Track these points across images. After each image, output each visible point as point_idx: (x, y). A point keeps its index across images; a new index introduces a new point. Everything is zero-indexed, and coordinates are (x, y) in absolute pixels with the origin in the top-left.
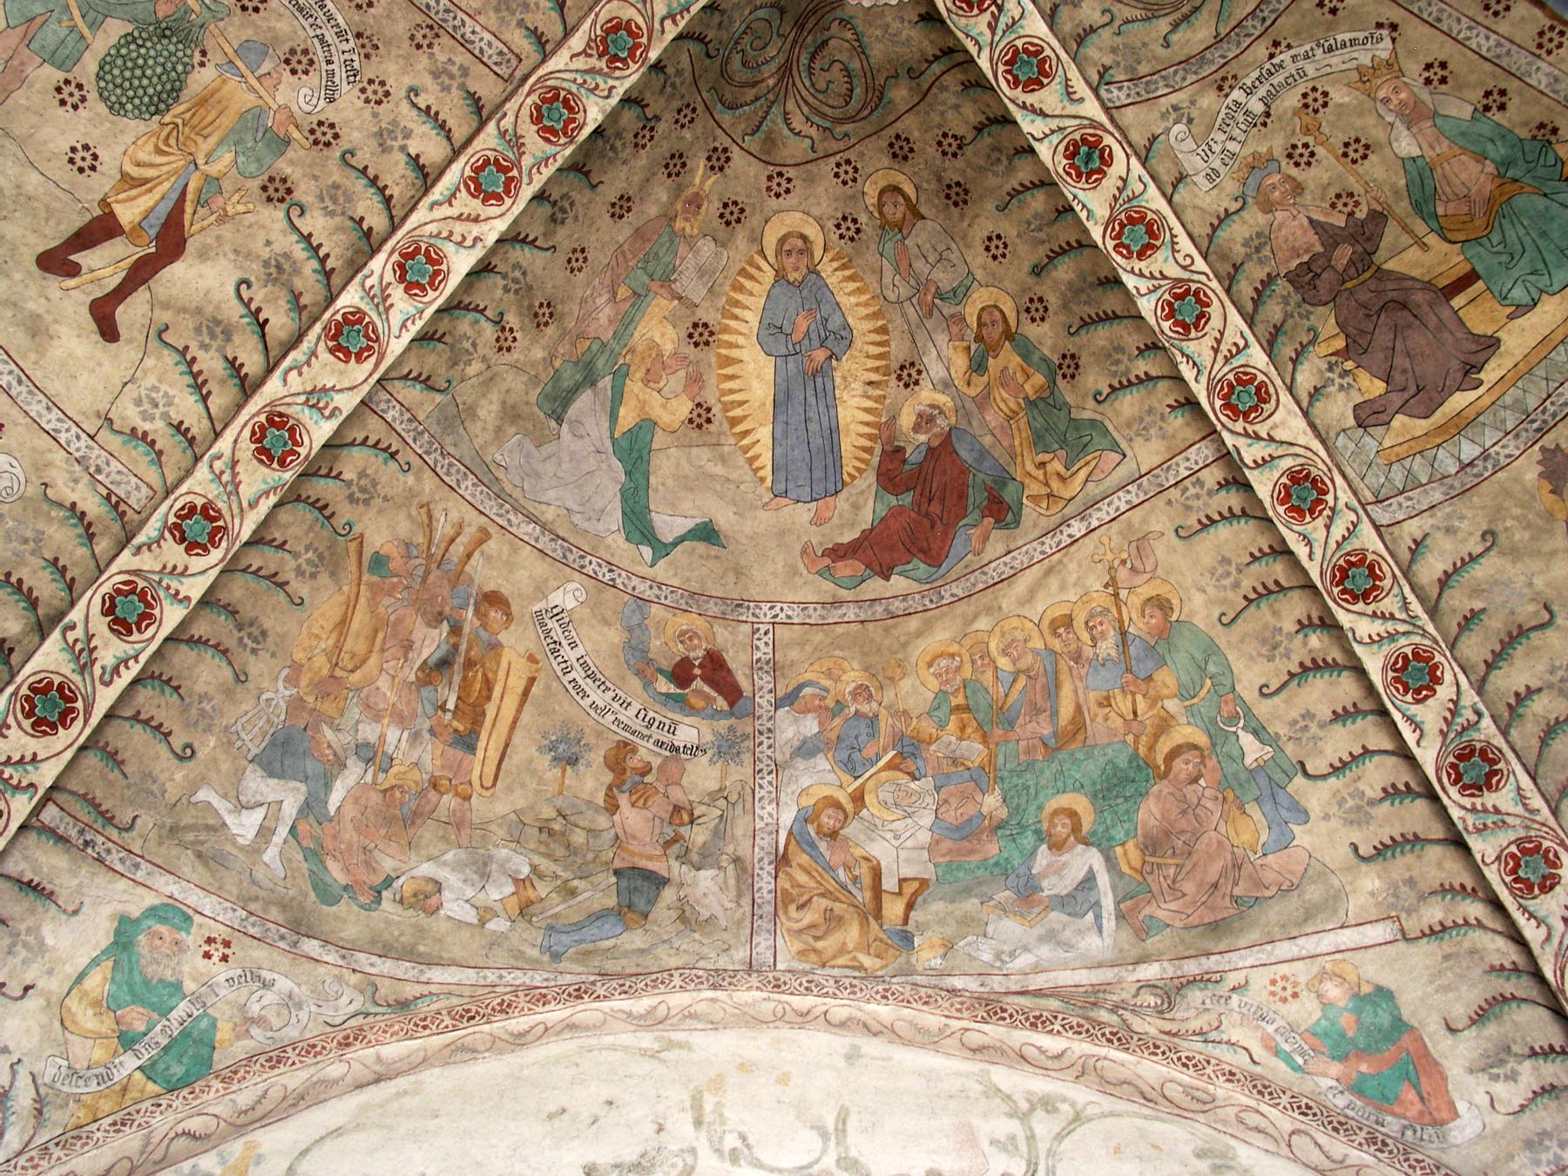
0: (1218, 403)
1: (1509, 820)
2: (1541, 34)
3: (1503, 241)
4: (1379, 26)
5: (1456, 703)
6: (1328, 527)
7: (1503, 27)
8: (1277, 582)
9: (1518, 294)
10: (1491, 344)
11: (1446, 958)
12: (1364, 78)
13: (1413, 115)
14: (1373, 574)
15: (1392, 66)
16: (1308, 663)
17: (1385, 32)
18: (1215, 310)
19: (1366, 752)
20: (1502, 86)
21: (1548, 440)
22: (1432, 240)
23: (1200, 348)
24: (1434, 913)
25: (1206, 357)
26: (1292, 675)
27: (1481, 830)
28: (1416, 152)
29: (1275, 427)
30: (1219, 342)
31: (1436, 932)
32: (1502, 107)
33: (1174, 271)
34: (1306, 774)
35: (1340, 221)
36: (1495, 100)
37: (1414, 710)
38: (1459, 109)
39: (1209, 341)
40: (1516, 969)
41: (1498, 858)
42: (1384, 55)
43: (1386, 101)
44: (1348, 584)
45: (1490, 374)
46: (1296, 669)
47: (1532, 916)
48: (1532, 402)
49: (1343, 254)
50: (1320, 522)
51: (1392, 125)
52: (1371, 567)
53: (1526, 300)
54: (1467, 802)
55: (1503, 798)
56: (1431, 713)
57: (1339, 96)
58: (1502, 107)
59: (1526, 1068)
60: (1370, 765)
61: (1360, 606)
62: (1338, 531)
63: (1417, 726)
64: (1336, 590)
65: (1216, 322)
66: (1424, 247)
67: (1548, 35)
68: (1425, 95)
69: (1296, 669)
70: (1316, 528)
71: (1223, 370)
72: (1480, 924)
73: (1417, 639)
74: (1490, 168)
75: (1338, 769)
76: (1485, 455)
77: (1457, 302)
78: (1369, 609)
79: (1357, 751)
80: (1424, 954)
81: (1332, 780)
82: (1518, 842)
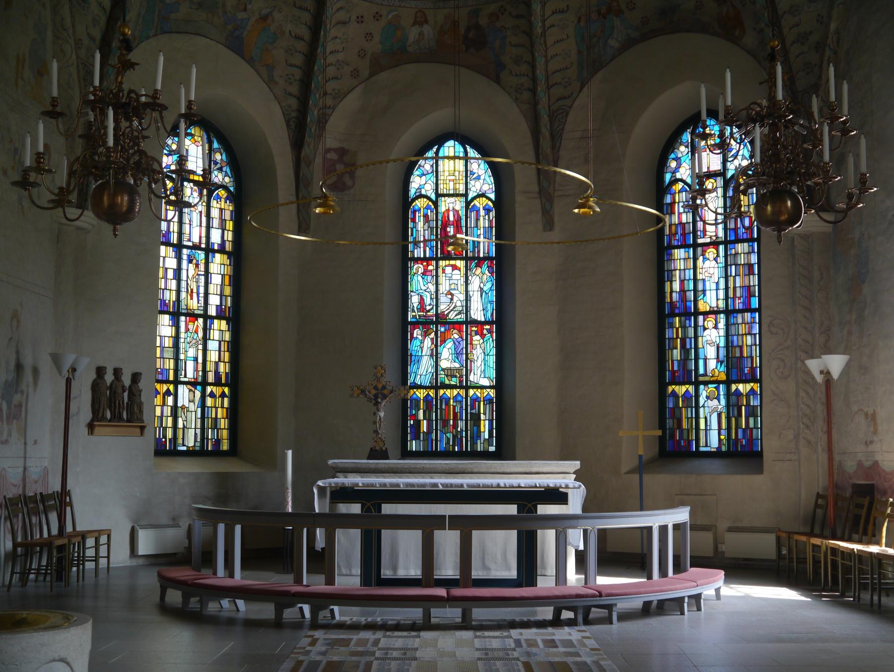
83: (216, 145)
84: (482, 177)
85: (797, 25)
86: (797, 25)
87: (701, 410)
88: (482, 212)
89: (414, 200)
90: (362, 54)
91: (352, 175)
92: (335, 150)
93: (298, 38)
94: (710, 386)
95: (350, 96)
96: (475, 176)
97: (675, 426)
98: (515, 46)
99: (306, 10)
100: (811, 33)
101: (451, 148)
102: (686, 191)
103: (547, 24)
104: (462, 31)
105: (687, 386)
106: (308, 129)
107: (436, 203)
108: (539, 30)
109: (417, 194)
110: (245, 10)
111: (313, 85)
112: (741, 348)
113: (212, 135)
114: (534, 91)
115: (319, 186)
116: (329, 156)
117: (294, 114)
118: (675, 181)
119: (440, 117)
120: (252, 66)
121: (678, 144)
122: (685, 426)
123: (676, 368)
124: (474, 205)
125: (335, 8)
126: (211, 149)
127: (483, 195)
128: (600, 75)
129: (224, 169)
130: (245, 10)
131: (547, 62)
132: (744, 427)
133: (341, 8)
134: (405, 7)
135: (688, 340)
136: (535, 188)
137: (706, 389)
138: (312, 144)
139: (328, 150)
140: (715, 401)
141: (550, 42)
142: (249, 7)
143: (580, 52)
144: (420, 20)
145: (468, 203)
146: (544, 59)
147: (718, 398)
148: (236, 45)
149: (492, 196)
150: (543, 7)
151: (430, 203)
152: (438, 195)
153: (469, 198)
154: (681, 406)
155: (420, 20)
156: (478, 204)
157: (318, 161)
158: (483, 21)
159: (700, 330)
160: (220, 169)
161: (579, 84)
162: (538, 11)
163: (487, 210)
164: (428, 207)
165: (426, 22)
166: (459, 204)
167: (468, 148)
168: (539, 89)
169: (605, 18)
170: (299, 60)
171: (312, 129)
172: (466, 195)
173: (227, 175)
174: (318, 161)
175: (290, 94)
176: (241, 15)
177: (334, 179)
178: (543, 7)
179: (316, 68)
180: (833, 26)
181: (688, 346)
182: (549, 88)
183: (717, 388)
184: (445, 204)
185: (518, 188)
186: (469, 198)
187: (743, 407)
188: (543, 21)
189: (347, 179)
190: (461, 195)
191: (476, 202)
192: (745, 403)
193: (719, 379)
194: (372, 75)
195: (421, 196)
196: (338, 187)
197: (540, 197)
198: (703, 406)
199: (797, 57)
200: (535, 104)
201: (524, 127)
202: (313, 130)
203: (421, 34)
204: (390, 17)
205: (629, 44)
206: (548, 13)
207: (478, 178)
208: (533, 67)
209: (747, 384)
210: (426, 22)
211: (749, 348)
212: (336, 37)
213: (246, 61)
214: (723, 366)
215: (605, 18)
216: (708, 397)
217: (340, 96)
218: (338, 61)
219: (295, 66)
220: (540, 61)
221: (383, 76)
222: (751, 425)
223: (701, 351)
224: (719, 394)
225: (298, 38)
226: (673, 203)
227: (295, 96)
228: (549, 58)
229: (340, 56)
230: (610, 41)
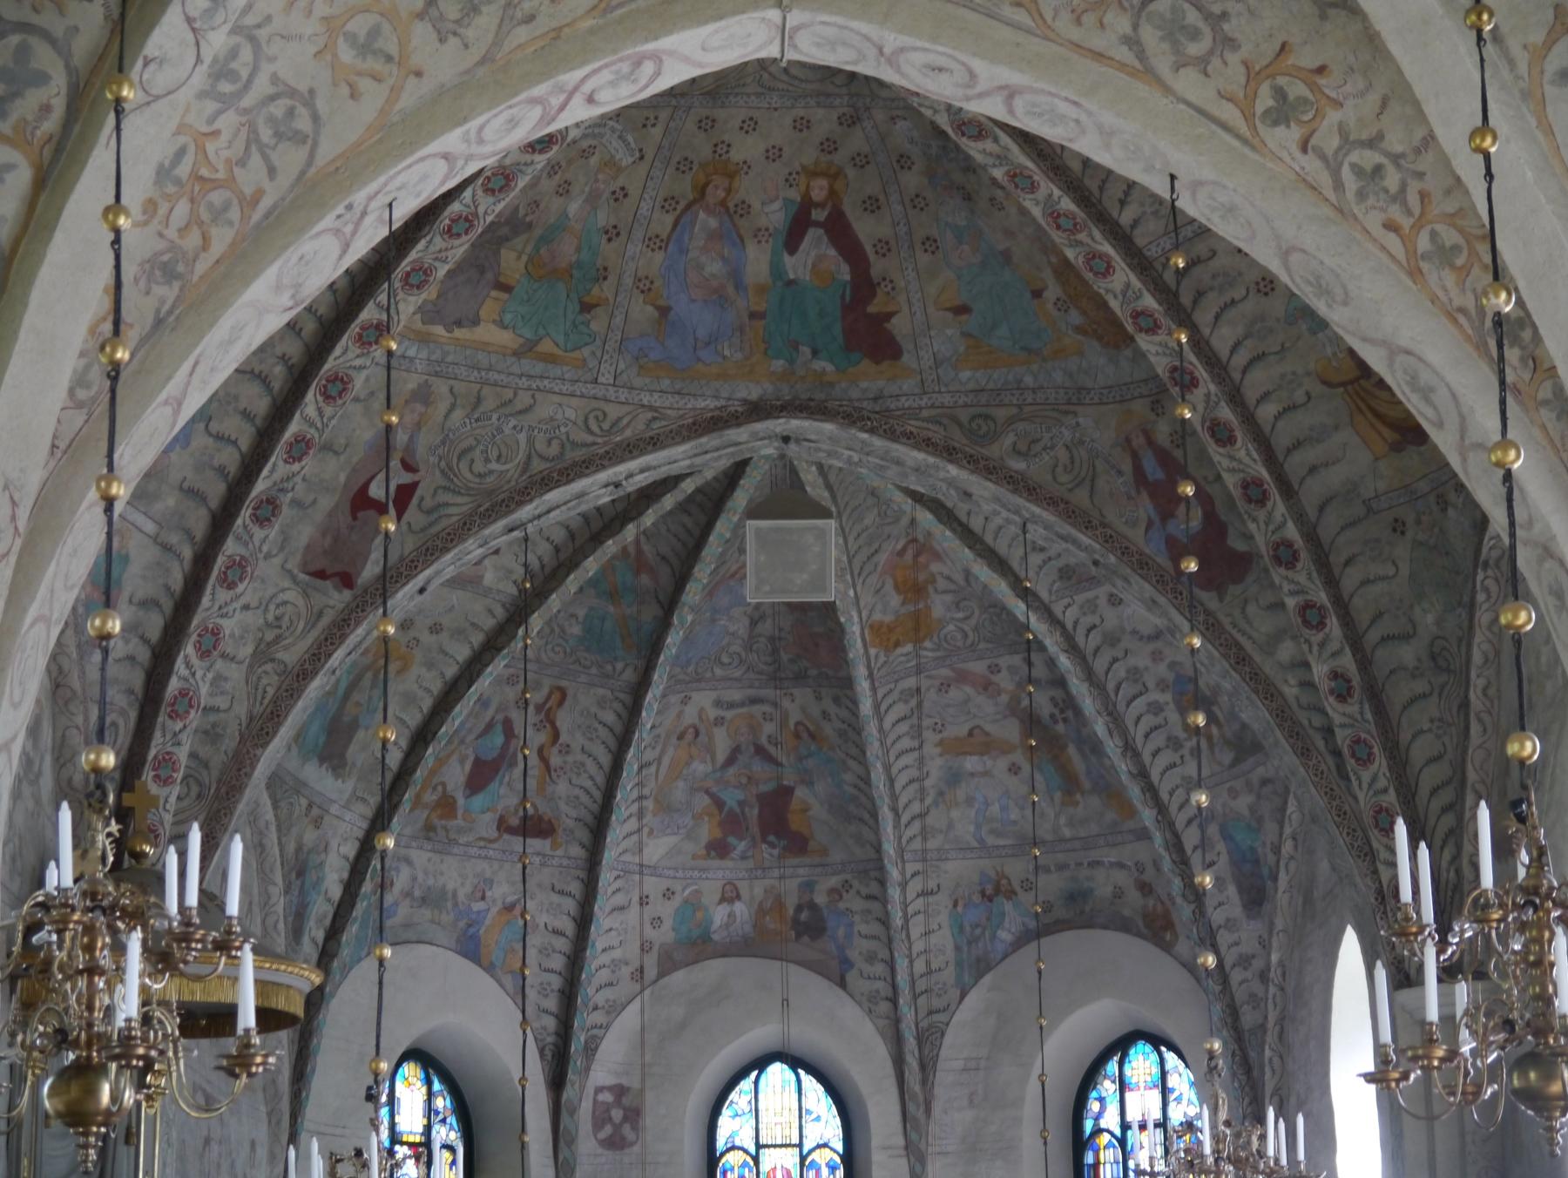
0: (408, 269)
1: (251, 546)
2: (657, 236)
3: (535, 291)
4: (641, 150)
5: (293, 475)
6: (358, 356)
7: (657, 215)
8: (301, 329)
9: (508, 317)
10: (476, 322)
11: (158, 564)
12: (610, 164)
13: (592, 199)
14: (340, 394)
15: (620, 170)
16: (263, 375)
17: (638, 155)
18: (464, 238)
19: (235, 443)
20: (622, 232)
21: (432, 379)
22: (525, 258)
23: (439, 242)
24: (174, 539)
25: (432, 249)
26: (252, 372)
27: (238, 538)
28: (571, 216)
29: (405, 300)
30: (446, 249)
31: (167, 548)
32: (610, 240)
33: (481, 210)
34: (207, 426)
35: (522, 212)
36: (612, 233)
37: (281, 463)
38: (603, 218)
39: (444, 245)
40: (172, 595)
41: (229, 557)
42: (624, 163)
43: (597, 181)
44: (329, 386)
45: (459, 333)
46: (257, 371)
47: (213, 594)
48: (450, 359)
49: (505, 230)
50: (358, 351)
51: (583, 192)
52: (344, 389)
53: (506, 322)
54: (248, 521)
55: (259, 533)
56: (283, 470)
57: (594, 161)
58: (610, 240)
59: (135, 640)
60: (230, 449)
61: (320, 399)
62: (358, 362)
63: (272, 471)
64: (324, 382)
65: (457, 242)
66: (519, 257)
67: (658, 241)
68: (606, 195)
69: (257, 371)
70: (355, 350)
71: (428, 260)
72: (182, 561)
73: (316, 435)
74: (574, 259)
75: (219, 437)
76: (412, 360)
77: (494, 293)
78: (321, 404)
79: (233, 438)
80: (153, 552)
81: (211, 440)
82: (242, 557)
83: (437, 1086)
84: (823, 1119)
85: (1237, 944)
86: (1237, 944)
88: (825, 1171)
89: (722, 1154)
90: (645, 947)
91: (635, 1128)
92: (610, 1089)
93: (556, 932)
95: (631, 1006)
96: (814, 1116)
98: (866, 937)
99: (569, 894)
100: (1253, 957)
101: (778, 1073)
102: (1114, 1147)
103: (910, 910)
104: (791, 911)
106: (572, 1063)
107: (756, 1159)
108: (898, 921)
109: (729, 1145)
110: (483, 898)
111: (579, 1000)
113: (431, 1071)
114: (894, 1001)
115: (587, 1146)
116: (601, 1097)
117: (550, 1039)
118: (1098, 1131)
119: (762, 1035)
120: (492, 976)
121: (1101, 1078)
124: (813, 1161)
125: (610, 891)
126: (430, 1095)
127: (825, 1145)
128: (987, 980)
129: (448, 1120)
130: (483, 898)
131: (911, 962)
133: (618, 890)
134: (707, 878)
136: (901, 1141)
138: (577, 1085)
139: (599, 1090)
141: (915, 932)
142: (489, 894)
143: (958, 948)
144: (730, 896)
145: (803, 1159)
146: (906, 961)
148: (470, 948)
149: (840, 1147)
150: (904, 891)
151: (749, 1159)
152: (759, 1146)
153: (805, 1151)
155: (730, 896)
156: (818, 1160)
157: (586, 1108)
158: (820, 899)
160: (444, 1121)
161: (958, 993)
162: (897, 897)
163: (833, 1169)
164: (745, 1164)
165: (738, 897)
166: (790, 1159)
167: (801, 1072)
168: (901, 1001)
169: (991, 900)
170: (558, 962)
171: (576, 1061)
172: (800, 1146)
173: (451, 1128)
174: (586, 1108)
175: (546, 1011)
176: (478, 906)
177: (608, 1130)
178: (904, 891)
179: (584, 976)
180: (1274, 958)
182: (915, 997)
184: (769, 1159)
185: (875, 1142)
186: (805, 1151)
188: (905, 905)
189: (627, 1130)
190: (794, 1146)
191: (815, 1156)
194: (662, 974)
195: (733, 1148)
196: (615, 1143)
197: (908, 1155)
199: (1240, 984)
200: (896, 1021)
201: (882, 1052)
202: (579, 1063)
203: (731, 915)
204: (687, 892)
205: (1026, 937)
206: (911, 895)
207: (818, 1119)
208: (892, 966)
210: (738, 897)
212: (611, 930)
213: (484, 969)
215: (991, 900)
217: (615, 1009)
218: (613, 961)
219: (552, 971)
220: (902, 964)
221: (678, 978)
225: (556, 932)
226: (1096, 1165)
227: (551, 1014)
228: (914, 956)
229: (617, 954)
230: (999, 932)
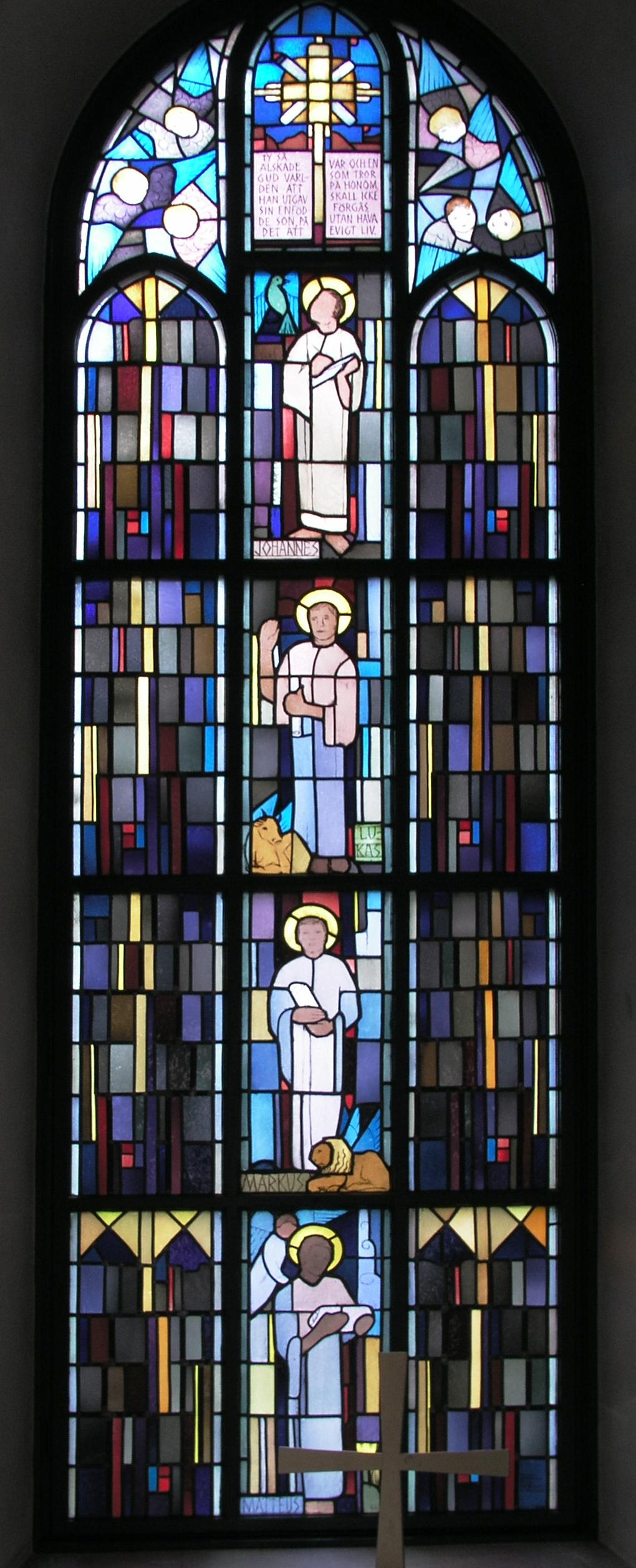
87: (259, 1327)
94: (304, 1216)
97: (116, 1404)
105: (184, 1217)
112: (472, 1048)
122: (166, 1400)
123: (122, 1131)
132: (475, 1403)
135: (191, 1006)
137: (285, 1229)
140: (333, 1290)
147: (348, 1275)
154: (147, 1306)
159: (251, 955)
181: (191, 1031)
183: (346, 1229)
187: (476, 1316)
192: (483, 1297)
193: (355, 1185)
198: (269, 1308)
209: (497, 1215)
211: (511, 1050)
214: (374, 1125)
216: (291, 1270)
222: (514, 1393)
223: (262, 1058)
224: (351, 1254)
